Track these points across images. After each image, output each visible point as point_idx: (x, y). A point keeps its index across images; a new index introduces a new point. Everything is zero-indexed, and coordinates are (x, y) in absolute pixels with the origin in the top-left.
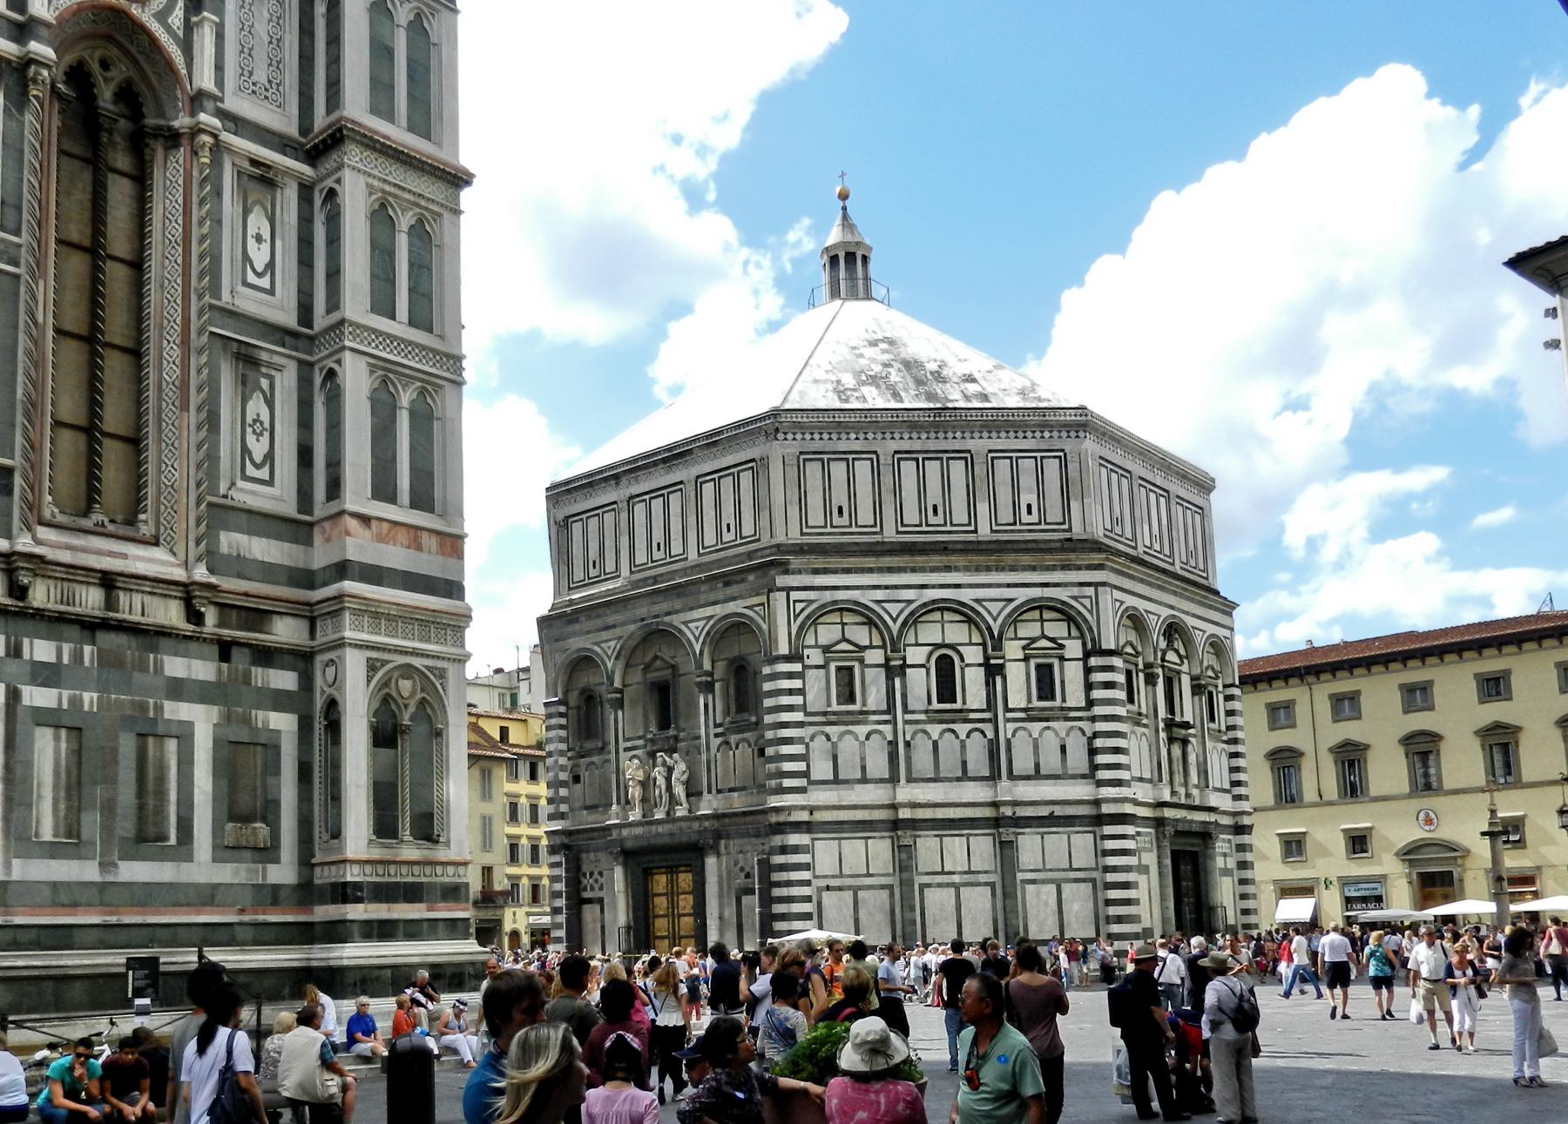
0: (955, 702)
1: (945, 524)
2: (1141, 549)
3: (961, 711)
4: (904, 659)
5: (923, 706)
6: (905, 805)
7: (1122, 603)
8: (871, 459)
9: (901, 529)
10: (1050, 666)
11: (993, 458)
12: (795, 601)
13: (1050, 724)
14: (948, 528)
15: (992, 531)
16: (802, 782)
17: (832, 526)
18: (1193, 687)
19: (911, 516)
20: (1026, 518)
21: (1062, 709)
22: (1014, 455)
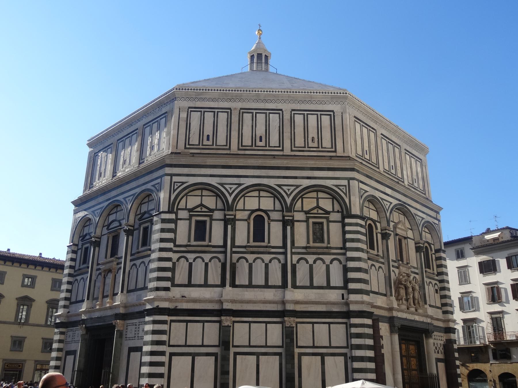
0: (264, 241)
1: (266, 146)
2: (381, 169)
3: (266, 247)
4: (235, 216)
5: (245, 243)
6: (227, 301)
7: (366, 191)
8: (227, 112)
9: (240, 147)
10: (322, 223)
11: (294, 114)
12: (175, 182)
13: (321, 256)
14: (267, 148)
15: (292, 150)
16: (168, 284)
17: (203, 145)
18: (416, 247)
19: (247, 141)
20: (311, 144)
21: (327, 248)
22: (306, 113)
